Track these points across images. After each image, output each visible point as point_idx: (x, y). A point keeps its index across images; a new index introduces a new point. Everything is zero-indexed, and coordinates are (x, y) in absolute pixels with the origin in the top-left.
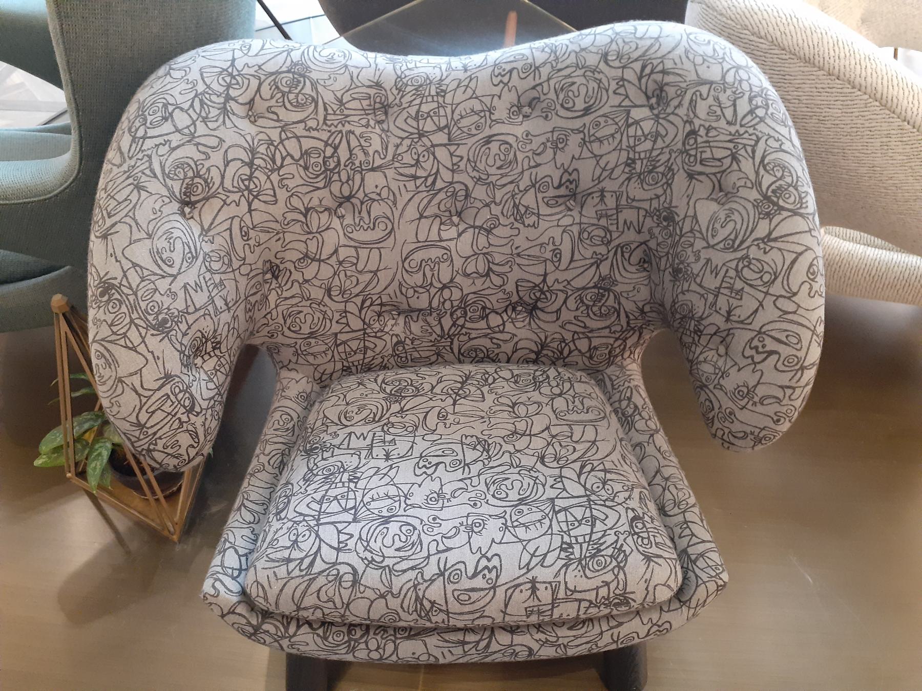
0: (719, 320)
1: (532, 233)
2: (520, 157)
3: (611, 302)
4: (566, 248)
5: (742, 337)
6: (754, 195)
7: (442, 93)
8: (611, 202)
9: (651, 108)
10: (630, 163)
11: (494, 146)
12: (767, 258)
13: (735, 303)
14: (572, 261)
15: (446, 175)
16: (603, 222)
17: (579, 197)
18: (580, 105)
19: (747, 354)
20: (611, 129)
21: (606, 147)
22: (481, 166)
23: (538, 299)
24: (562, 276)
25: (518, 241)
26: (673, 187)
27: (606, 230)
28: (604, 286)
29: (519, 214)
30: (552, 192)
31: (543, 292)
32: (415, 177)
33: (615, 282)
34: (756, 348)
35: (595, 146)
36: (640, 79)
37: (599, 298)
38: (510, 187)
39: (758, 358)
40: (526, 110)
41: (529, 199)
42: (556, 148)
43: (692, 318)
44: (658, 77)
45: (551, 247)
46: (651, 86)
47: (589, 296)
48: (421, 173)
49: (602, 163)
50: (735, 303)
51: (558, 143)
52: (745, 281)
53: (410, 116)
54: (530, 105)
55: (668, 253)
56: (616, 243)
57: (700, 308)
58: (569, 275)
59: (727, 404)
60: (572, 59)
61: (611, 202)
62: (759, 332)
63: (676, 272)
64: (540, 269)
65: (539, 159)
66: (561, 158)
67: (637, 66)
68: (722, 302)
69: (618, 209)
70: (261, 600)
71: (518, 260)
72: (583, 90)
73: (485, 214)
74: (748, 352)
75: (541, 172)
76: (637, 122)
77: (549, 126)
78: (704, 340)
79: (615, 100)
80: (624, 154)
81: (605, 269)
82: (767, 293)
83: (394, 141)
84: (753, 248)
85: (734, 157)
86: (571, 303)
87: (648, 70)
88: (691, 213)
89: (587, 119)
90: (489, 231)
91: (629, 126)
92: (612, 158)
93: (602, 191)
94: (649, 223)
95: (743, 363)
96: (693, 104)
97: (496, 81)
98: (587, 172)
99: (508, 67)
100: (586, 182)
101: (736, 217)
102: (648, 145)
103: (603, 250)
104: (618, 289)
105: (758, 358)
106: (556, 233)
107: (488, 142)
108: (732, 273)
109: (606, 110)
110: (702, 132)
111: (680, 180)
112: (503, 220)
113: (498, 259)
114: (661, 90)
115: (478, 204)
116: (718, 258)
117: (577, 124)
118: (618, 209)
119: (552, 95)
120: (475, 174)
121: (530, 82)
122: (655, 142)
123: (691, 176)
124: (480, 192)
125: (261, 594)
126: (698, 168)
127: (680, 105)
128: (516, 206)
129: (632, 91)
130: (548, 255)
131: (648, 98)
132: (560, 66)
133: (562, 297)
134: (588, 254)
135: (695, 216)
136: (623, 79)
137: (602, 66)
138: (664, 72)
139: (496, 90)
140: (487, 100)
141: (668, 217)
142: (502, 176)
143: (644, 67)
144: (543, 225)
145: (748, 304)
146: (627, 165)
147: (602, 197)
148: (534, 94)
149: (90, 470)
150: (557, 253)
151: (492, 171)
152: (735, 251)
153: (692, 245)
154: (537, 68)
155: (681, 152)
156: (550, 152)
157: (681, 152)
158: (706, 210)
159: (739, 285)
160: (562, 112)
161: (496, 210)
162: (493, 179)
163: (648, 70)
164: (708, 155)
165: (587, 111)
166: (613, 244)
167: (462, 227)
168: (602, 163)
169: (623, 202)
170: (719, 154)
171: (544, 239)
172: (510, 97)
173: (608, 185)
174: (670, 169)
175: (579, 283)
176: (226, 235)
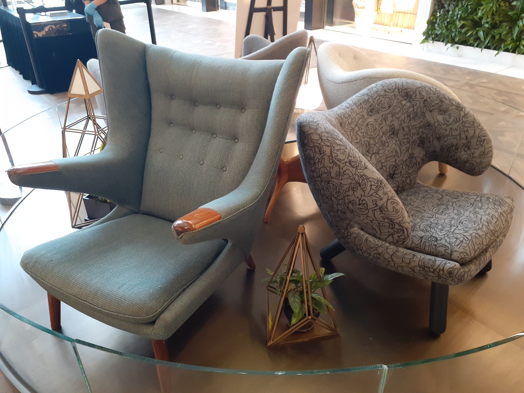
0: (464, 141)
1: (388, 149)
2: (377, 127)
3: (414, 161)
4: (398, 149)
5: (474, 141)
6: (454, 107)
7: (349, 116)
8: (406, 129)
9: (405, 100)
10: (409, 116)
11: (369, 126)
12: (468, 119)
13: (467, 134)
14: (401, 152)
15: (362, 139)
16: (406, 137)
17: (395, 133)
18: (387, 106)
19: (478, 143)
20: (399, 109)
21: (400, 114)
22: (369, 133)
23: (395, 170)
24: (400, 159)
25: (386, 152)
26: (426, 116)
27: (408, 138)
28: (411, 157)
29: (383, 144)
30: (389, 134)
31: (396, 167)
32: (358, 143)
33: (414, 154)
34: (480, 141)
35: (396, 115)
36: (399, 93)
37: (411, 161)
38: (378, 137)
39: (482, 143)
40: (370, 113)
41: (384, 139)
42: (385, 120)
43: (453, 146)
44: (405, 91)
45: (394, 151)
46: (403, 94)
47: (408, 161)
48: (358, 141)
49: (400, 119)
50: (467, 134)
51: (385, 119)
52: (467, 127)
53: (416, 105)
54: (370, 112)
55: (432, 135)
56: (411, 142)
57: (455, 142)
58: (401, 158)
59: (478, 160)
60: (376, 95)
61: (406, 129)
62: (479, 137)
63: (439, 139)
64: (394, 160)
65: (382, 126)
66: (388, 123)
67: (397, 90)
68: (463, 136)
69: (410, 131)
70: (466, 256)
71: (388, 159)
72: (386, 102)
73: (375, 149)
74: (478, 143)
75: (384, 129)
76: (405, 105)
77: (380, 115)
78: (459, 150)
79: (396, 101)
80: (406, 115)
81: (410, 151)
82: (475, 127)
83: (349, 133)
84: (464, 119)
85: (442, 101)
86: (404, 167)
87: (400, 90)
88: (436, 120)
89: (391, 109)
90: (378, 153)
91: (403, 106)
92: (403, 117)
93: (403, 128)
94: (421, 130)
95: (478, 147)
96: (420, 94)
97: (359, 107)
98: (396, 124)
99: (359, 103)
100: (397, 127)
101: (452, 114)
102: (412, 109)
103: (408, 145)
104: (415, 156)
105: (482, 143)
106: (394, 146)
107: (367, 126)
108: (462, 127)
109: (395, 104)
110: (428, 99)
111: (428, 114)
112: (380, 148)
113: (383, 161)
114: (407, 94)
115: (373, 146)
116: (454, 126)
117: (389, 111)
118: (410, 131)
119: (377, 106)
120: (369, 136)
121: (368, 105)
122: (413, 107)
123: (431, 111)
124: (372, 142)
125: (465, 254)
126: (432, 108)
127: (416, 95)
128: (382, 142)
129: (399, 97)
130: (395, 154)
131: (403, 98)
132: (374, 98)
133: (401, 166)
134: (404, 148)
135: (438, 121)
136: (395, 95)
137: (387, 93)
138: (405, 89)
139: (361, 110)
140: (361, 113)
141: (429, 125)
142: (375, 134)
143: (399, 90)
144: (390, 145)
145: (471, 132)
146: (408, 117)
147: (403, 129)
148: (371, 108)
149: (420, 235)
150: (396, 152)
151: (372, 134)
152: (459, 122)
153: (441, 128)
154: (368, 100)
155: (425, 106)
156: (384, 122)
157: (425, 106)
158: (440, 118)
159: (465, 129)
160: (383, 110)
161: (377, 145)
162: (373, 136)
163: (400, 90)
164: (433, 104)
165: (390, 107)
166: (411, 142)
167: (370, 156)
168: (400, 119)
169: (411, 128)
170: (437, 102)
171: (392, 149)
172: (365, 111)
173: (404, 125)
174: (423, 112)
175: (404, 160)
176: (402, 151)
